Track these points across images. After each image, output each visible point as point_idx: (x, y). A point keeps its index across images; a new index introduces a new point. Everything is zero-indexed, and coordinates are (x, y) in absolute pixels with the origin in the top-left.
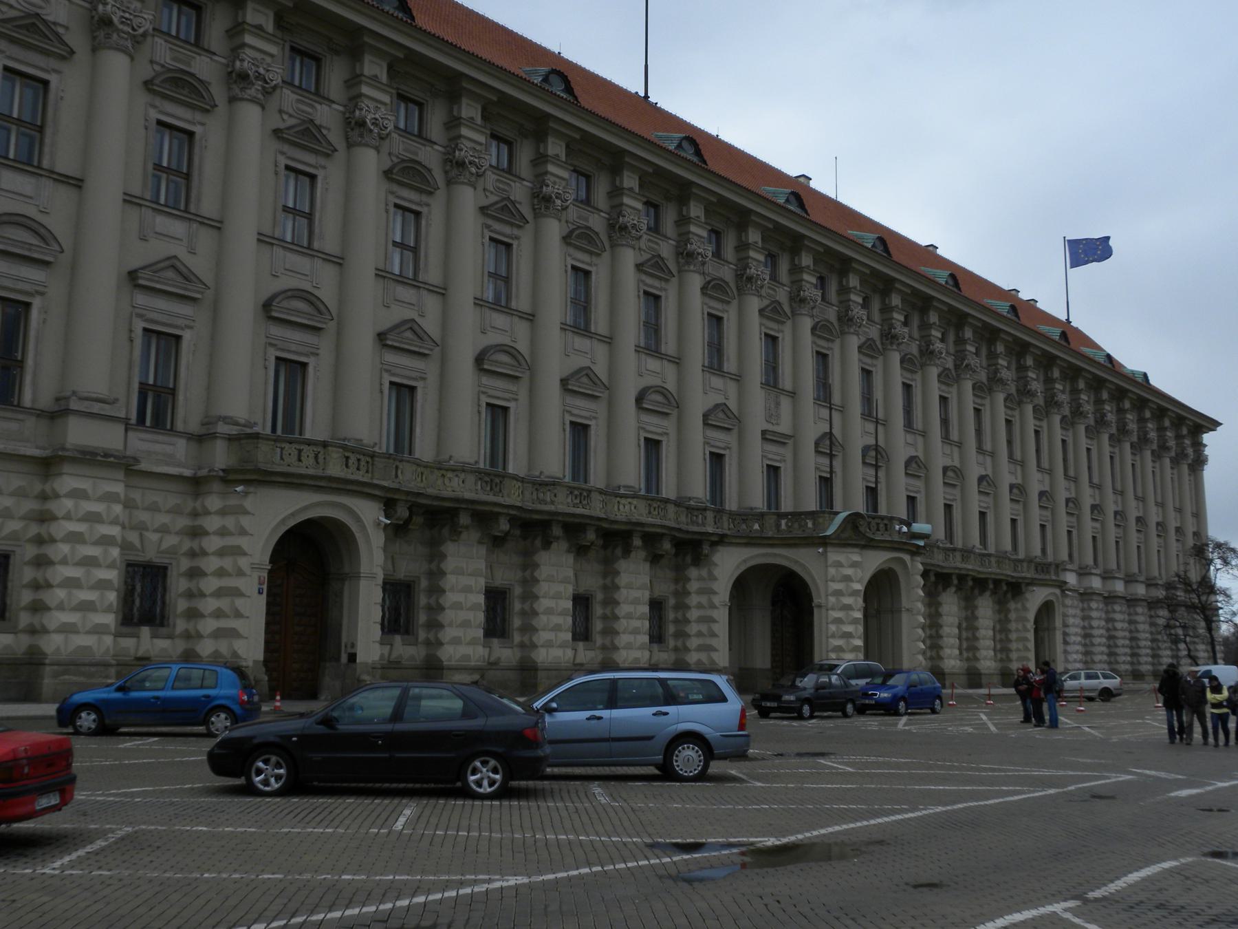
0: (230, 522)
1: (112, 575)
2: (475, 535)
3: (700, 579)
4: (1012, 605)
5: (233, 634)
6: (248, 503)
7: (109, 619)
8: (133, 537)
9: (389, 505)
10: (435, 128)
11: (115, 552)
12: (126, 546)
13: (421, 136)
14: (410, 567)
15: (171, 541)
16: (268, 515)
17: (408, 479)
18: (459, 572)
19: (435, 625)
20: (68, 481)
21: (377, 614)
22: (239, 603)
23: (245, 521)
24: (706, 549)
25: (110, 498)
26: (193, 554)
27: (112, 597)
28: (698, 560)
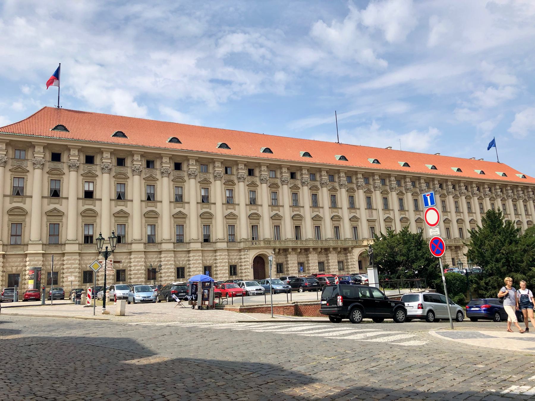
0: (245, 256)
1: (227, 268)
2: (294, 253)
3: (350, 256)
4: (459, 252)
5: (248, 276)
6: (248, 253)
7: (227, 275)
8: (230, 261)
9: (274, 250)
10: (279, 176)
11: (227, 264)
12: (229, 262)
13: (276, 178)
14: (281, 260)
15: (236, 261)
16: (252, 255)
17: (278, 245)
18: (291, 260)
19: (288, 271)
20: (218, 254)
21: (275, 270)
22: (248, 270)
23: (248, 256)
24: (350, 249)
25: (225, 255)
26: (240, 262)
27: (227, 271)
28: (350, 252)
